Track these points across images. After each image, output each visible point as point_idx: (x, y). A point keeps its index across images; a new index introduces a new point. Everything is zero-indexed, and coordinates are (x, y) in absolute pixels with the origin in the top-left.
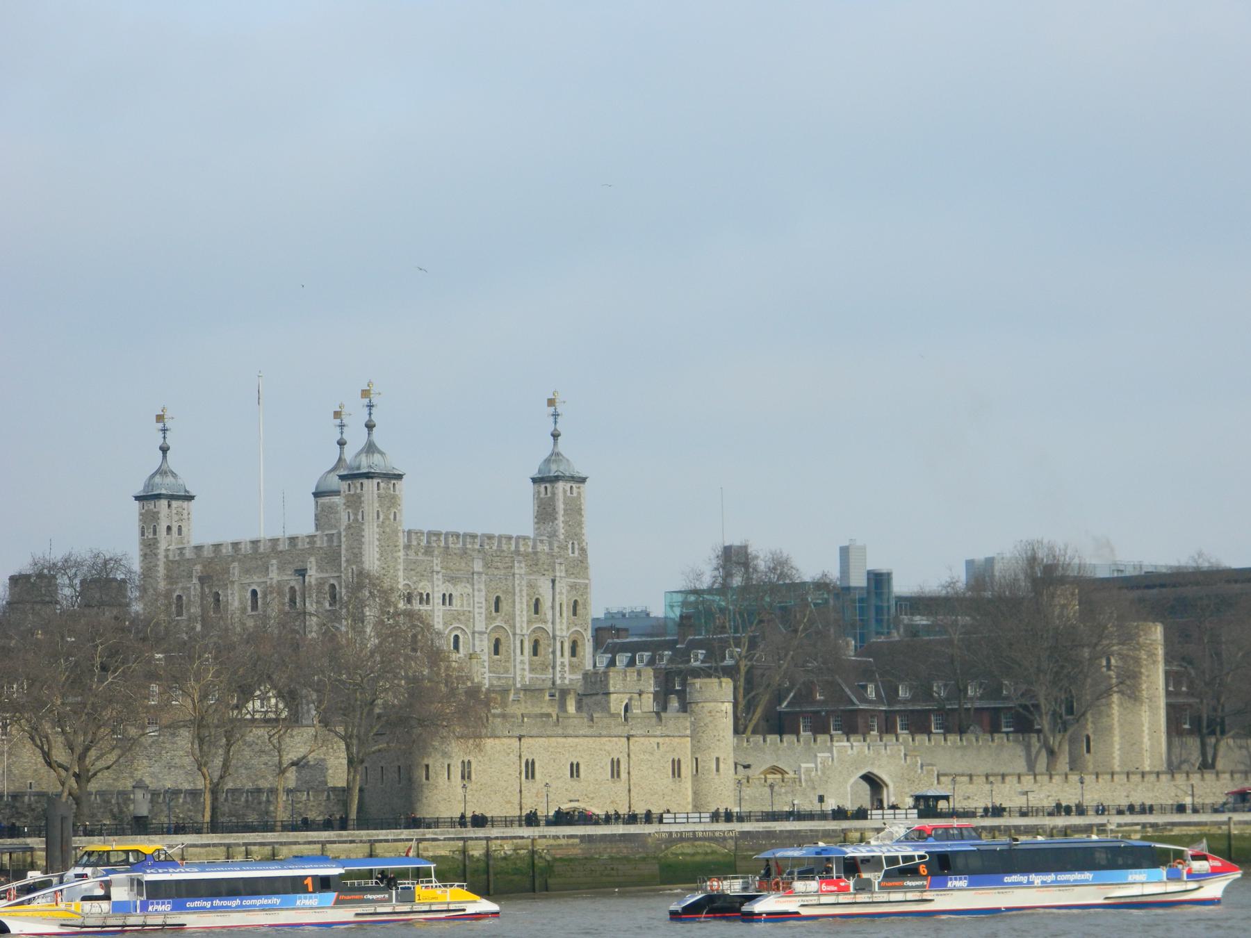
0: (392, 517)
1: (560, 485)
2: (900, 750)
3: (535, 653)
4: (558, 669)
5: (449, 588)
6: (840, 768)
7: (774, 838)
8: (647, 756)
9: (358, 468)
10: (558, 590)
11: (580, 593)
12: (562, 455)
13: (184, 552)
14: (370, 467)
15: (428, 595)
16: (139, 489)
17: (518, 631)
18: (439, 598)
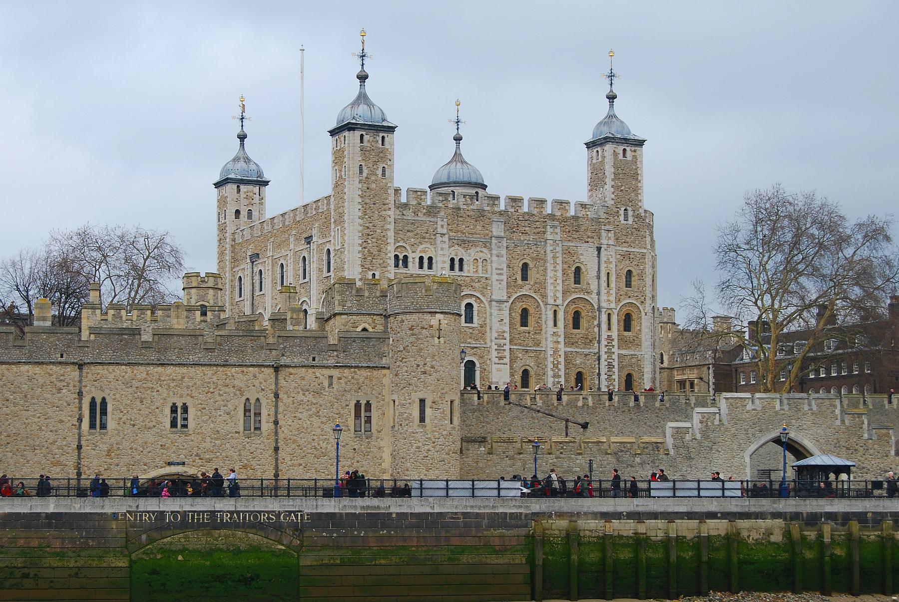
0: (380, 172)
1: (609, 147)
3: (576, 325)
4: (604, 342)
5: (459, 252)
6: (733, 430)
7: (383, 528)
8: (310, 397)
10: (603, 258)
11: (636, 263)
12: (616, 117)
13: (244, 233)
15: (430, 259)
16: (217, 179)
17: (551, 301)
18: (444, 262)
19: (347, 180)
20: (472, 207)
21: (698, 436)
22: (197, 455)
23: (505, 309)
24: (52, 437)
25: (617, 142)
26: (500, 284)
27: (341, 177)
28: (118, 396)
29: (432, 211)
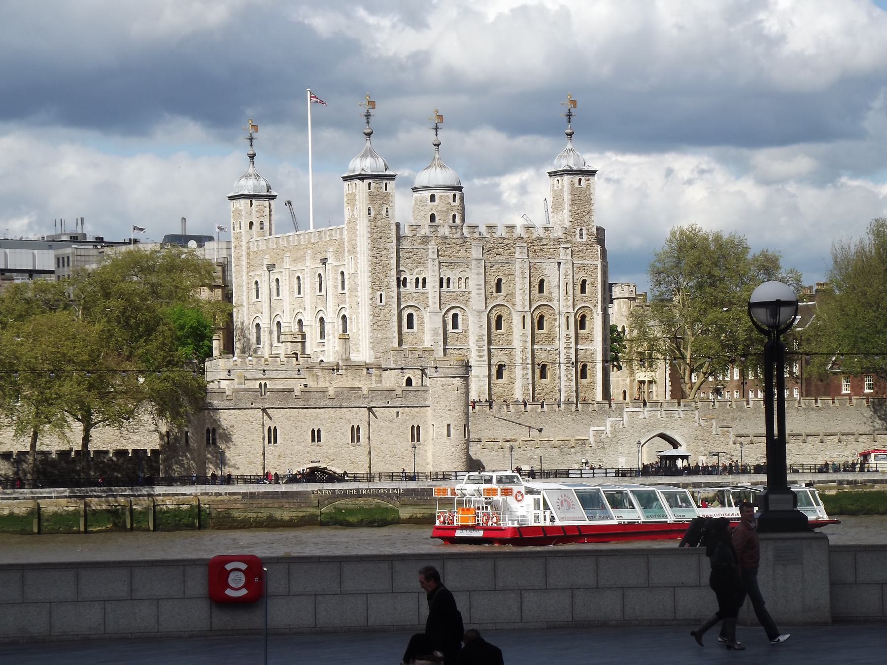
0: (384, 212)
1: (567, 179)
2: (695, 415)
6: (631, 431)
9: (354, 171)
13: (260, 243)
14: (363, 170)
18: (435, 281)
19: (358, 219)
20: (456, 236)
21: (609, 435)
22: (327, 457)
23: (484, 317)
24: (248, 449)
25: (574, 174)
26: (480, 297)
27: (353, 215)
28: (283, 425)
29: (425, 240)
